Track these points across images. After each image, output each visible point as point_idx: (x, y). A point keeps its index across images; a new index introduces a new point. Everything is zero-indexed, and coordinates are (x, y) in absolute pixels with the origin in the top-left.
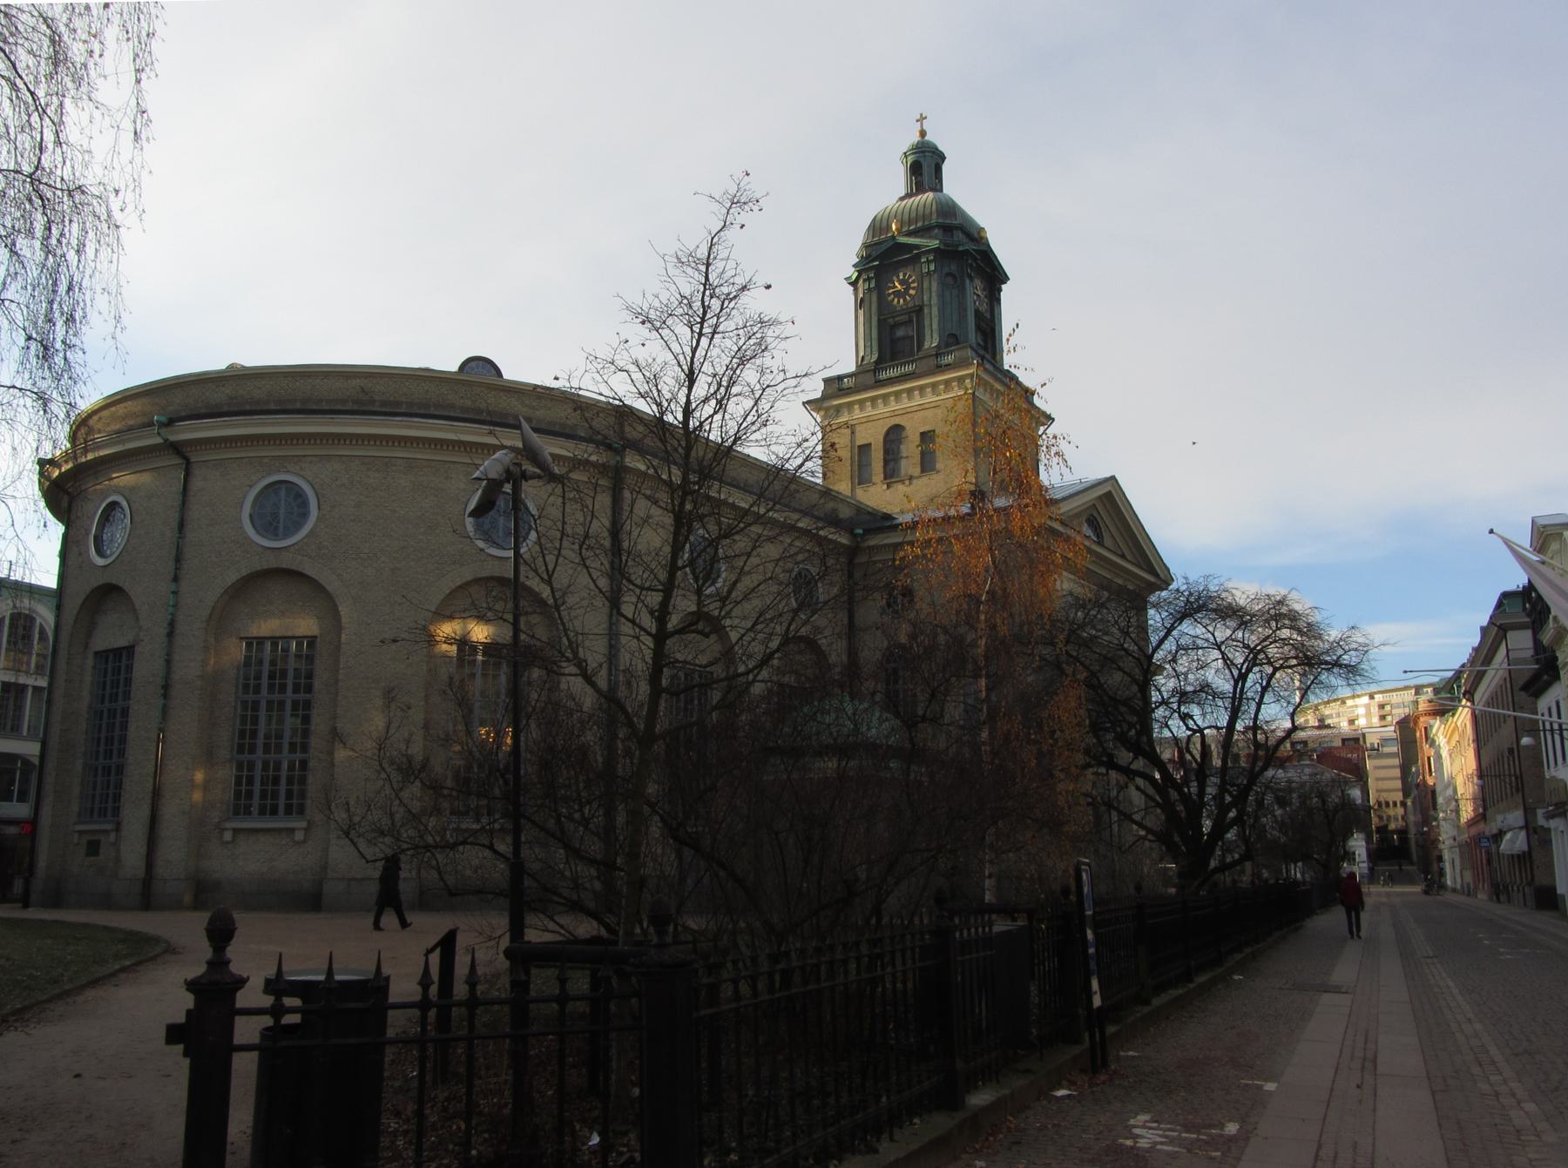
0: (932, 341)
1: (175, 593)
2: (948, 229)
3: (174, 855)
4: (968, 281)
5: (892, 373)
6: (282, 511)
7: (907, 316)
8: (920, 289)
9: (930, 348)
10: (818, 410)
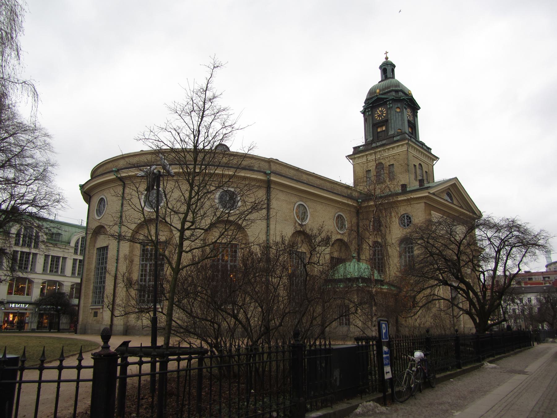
5: (378, 144)
8: (387, 114)
10: (351, 159)
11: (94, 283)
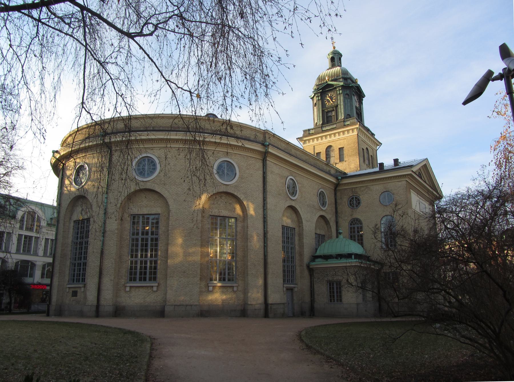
0: (341, 116)
2: (345, 79)
3: (107, 296)
4: (353, 97)
6: (146, 168)
7: (332, 109)
9: (341, 119)
10: (302, 141)
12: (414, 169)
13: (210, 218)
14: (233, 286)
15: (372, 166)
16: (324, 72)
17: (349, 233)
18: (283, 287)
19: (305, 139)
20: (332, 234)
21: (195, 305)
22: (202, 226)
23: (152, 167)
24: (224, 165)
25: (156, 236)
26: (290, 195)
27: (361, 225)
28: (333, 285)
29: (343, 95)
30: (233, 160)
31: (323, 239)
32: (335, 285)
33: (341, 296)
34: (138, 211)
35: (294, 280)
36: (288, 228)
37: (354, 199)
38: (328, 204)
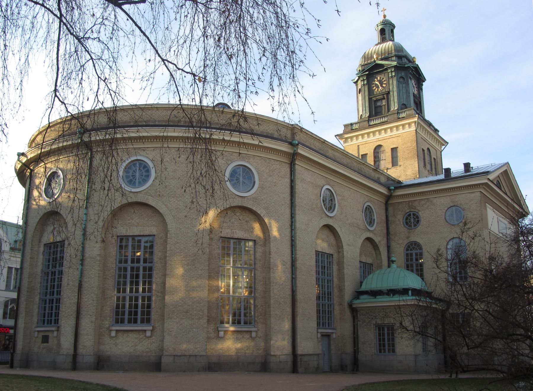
0: (394, 107)
1: (86, 214)
4: (410, 80)
6: (137, 174)
7: (382, 96)
9: (394, 110)
11: (40, 293)
12: (492, 177)
13: (221, 241)
14: (251, 331)
15: (436, 172)
16: (372, 49)
17: (404, 261)
18: (318, 332)
19: (346, 136)
20: (382, 262)
21: (201, 356)
22: (209, 251)
23: (144, 174)
24: (238, 170)
25: (150, 265)
26: (326, 209)
27: (421, 251)
28: (383, 330)
29: (397, 79)
30: (251, 165)
31: (370, 269)
32: (386, 329)
33: (393, 345)
34: (127, 231)
35: (331, 323)
36: (324, 255)
37: (412, 216)
38: (377, 223)
